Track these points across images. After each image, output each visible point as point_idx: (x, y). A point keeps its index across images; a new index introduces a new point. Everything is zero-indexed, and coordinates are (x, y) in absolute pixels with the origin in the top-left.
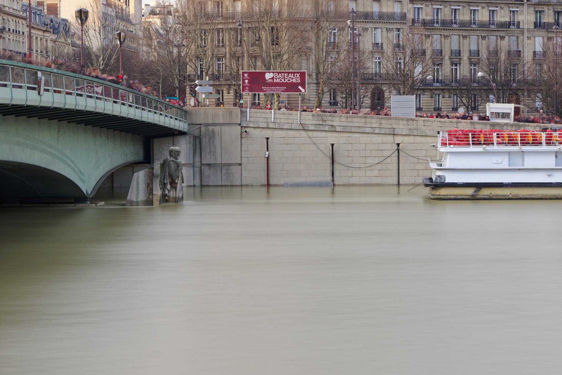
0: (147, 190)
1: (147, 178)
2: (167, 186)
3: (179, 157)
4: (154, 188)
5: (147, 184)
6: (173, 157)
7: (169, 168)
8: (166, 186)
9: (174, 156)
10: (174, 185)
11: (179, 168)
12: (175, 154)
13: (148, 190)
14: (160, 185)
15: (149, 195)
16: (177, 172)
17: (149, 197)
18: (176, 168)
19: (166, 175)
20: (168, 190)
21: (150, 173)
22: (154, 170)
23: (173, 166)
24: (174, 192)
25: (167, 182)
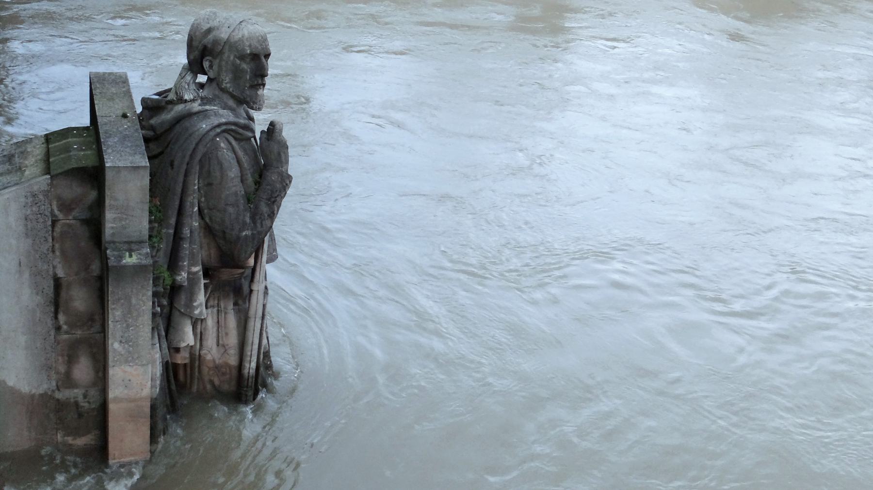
0: (50, 322)
1: (45, 247)
2: (191, 298)
3: (260, 92)
4: (115, 346)
5: (48, 286)
6: (224, 90)
7: (209, 185)
8: (182, 298)
9: (227, 81)
10: (226, 274)
11: (272, 177)
12: (237, 73)
13: (58, 328)
14: (154, 315)
15: (71, 360)
16: (264, 209)
17: (68, 375)
18: (250, 180)
19: (186, 232)
20: (191, 318)
21: (66, 207)
22: (109, 215)
23: (233, 172)
24: (232, 321)
25: (189, 273)
